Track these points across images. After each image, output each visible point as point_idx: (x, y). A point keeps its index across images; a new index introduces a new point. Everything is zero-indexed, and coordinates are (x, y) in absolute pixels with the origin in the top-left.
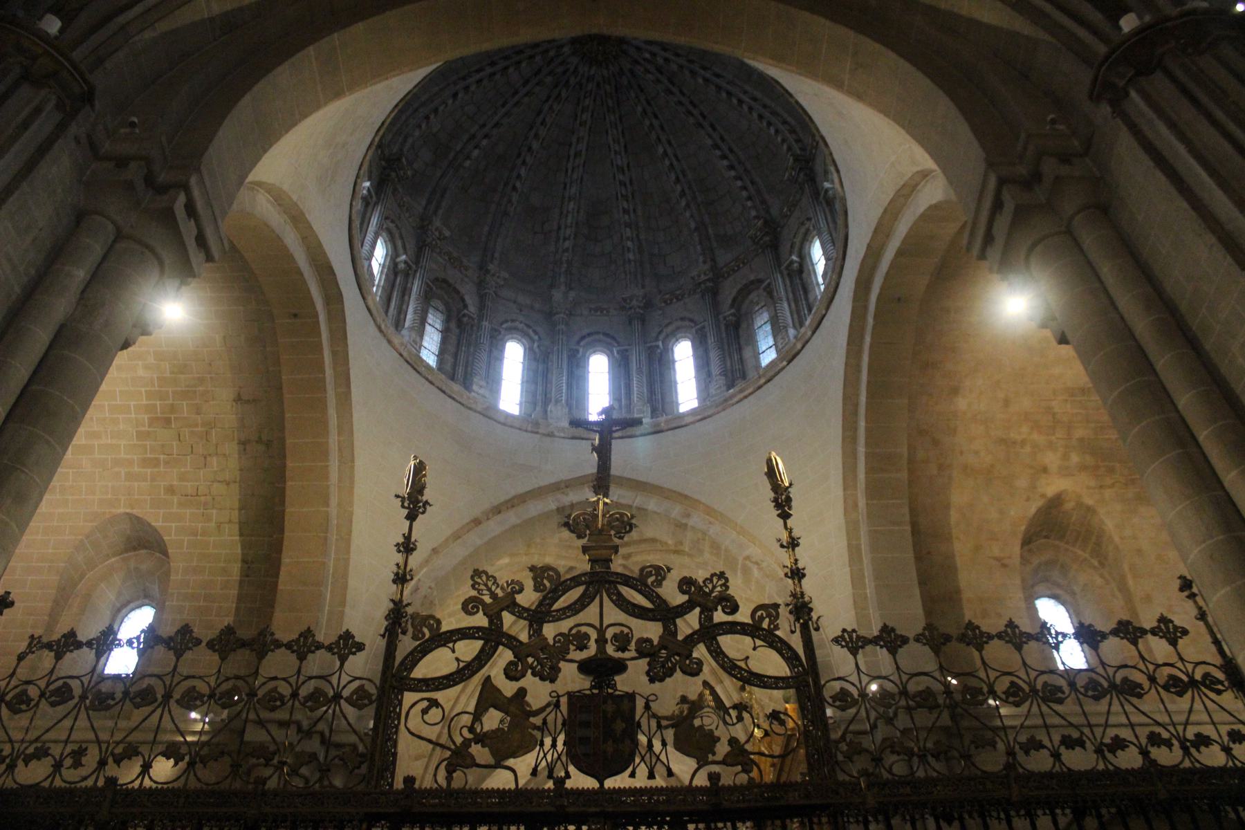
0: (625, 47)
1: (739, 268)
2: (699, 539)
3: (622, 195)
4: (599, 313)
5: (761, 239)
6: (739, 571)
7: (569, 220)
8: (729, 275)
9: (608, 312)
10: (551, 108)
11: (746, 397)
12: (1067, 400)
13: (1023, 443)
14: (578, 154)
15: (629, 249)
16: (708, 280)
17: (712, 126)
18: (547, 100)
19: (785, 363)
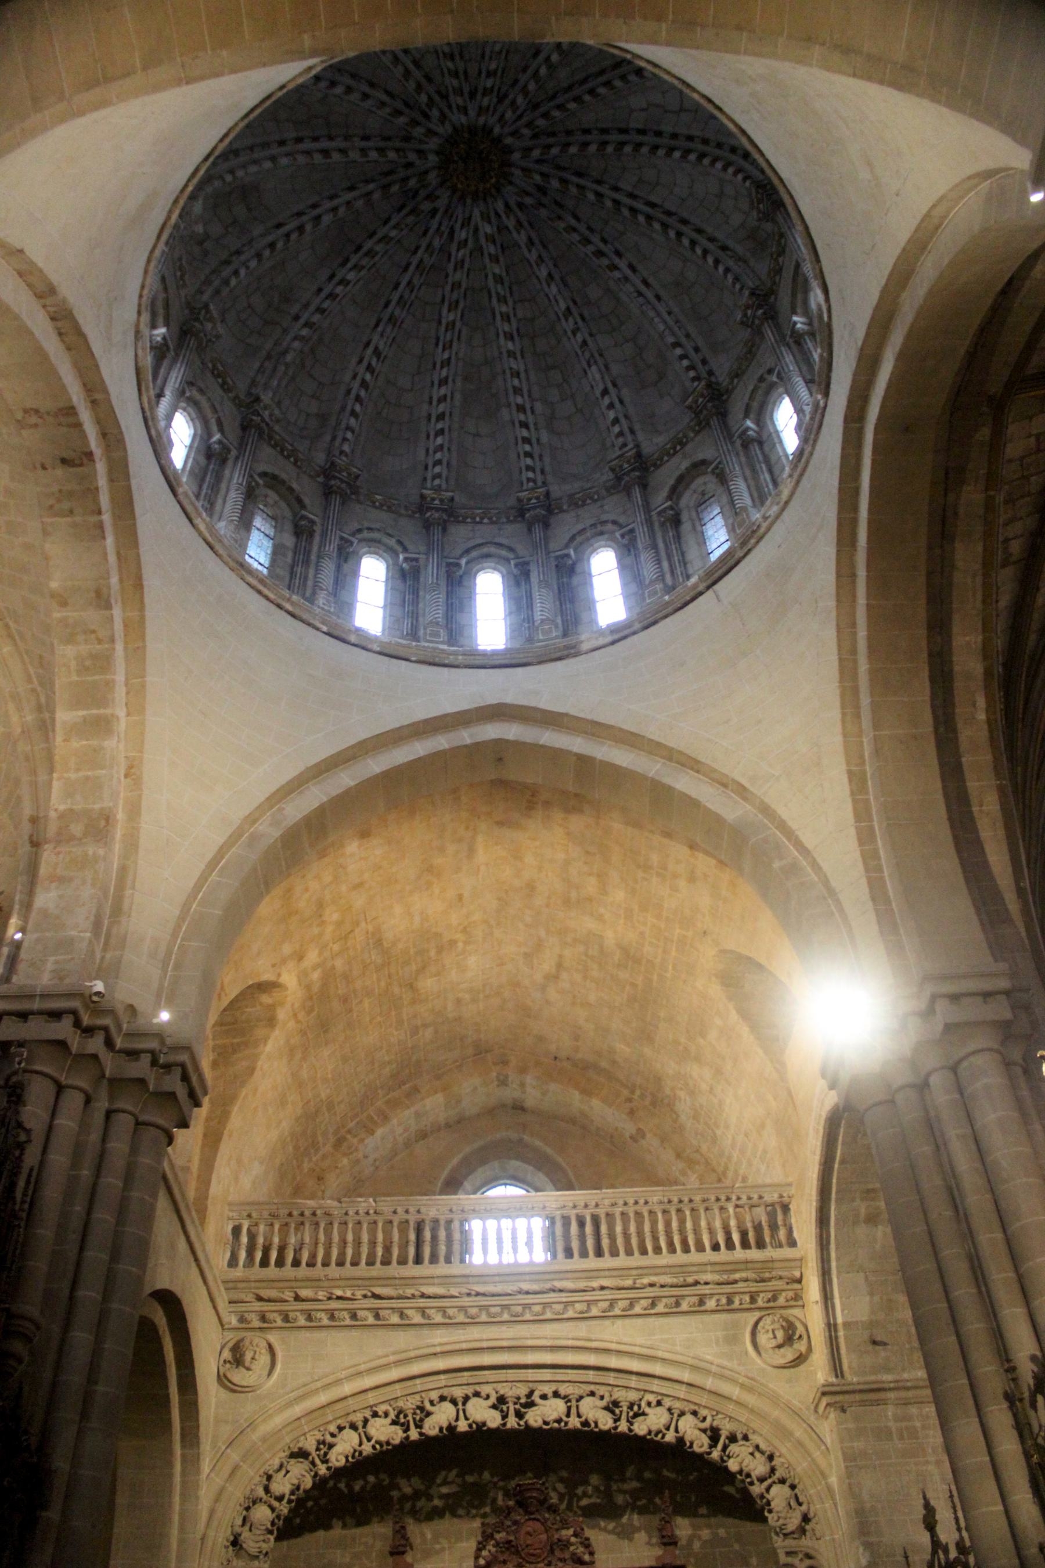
0: (469, 201)
1: (288, 457)
2: (93, 632)
3: (288, 235)
4: (179, 274)
5: (342, 481)
6: (82, 713)
7: (253, 169)
8: (274, 447)
9: (185, 285)
10: (383, 104)
11: (259, 592)
12: (367, 933)
13: (323, 922)
14: (326, 153)
15: (236, 273)
16: (267, 425)
17: (394, 338)
18: (388, 93)
19: (325, 629)
